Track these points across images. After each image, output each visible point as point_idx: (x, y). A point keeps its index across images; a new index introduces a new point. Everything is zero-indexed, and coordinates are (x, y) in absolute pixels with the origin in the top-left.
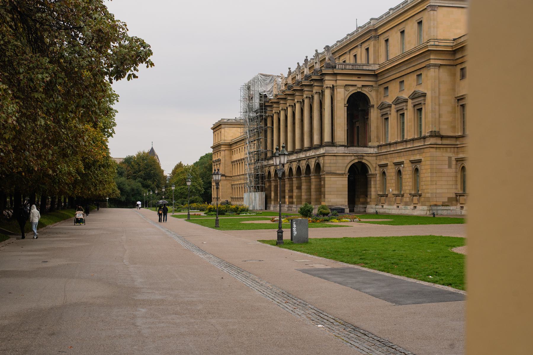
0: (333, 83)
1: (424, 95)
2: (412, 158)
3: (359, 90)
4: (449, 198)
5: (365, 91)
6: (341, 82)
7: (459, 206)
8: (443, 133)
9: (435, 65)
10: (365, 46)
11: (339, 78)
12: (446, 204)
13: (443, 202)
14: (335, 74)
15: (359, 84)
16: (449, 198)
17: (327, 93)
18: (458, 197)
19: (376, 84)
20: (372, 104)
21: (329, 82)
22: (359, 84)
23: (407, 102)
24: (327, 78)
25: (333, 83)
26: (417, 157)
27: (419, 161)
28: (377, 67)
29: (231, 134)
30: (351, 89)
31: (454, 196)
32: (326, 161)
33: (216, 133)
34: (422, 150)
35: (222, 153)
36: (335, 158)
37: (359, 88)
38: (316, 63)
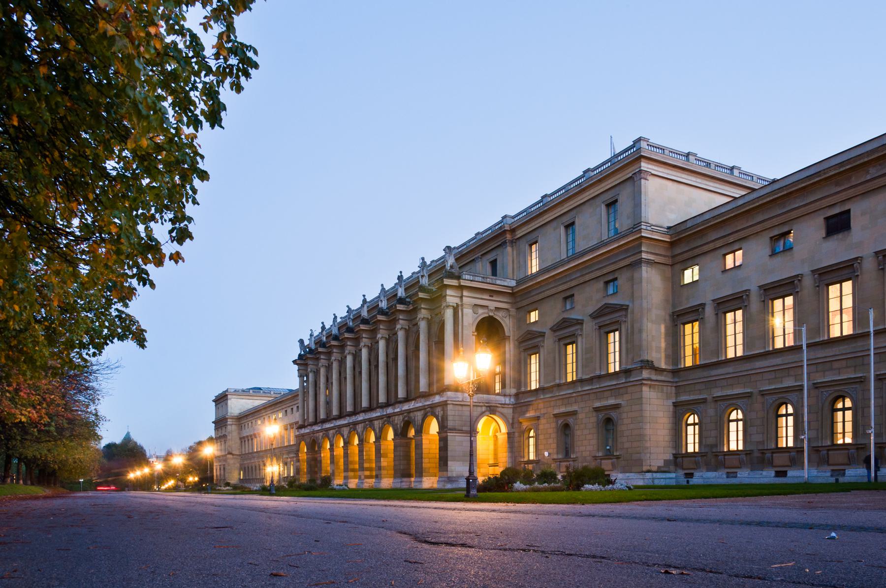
0: (457, 300)
1: (624, 308)
2: (597, 404)
3: (491, 314)
4: (665, 461)
5: (499, 316)
6: (469, 299)
7: (681, 473)
8: (656, 364)
9: (649, 262)
10: (491, 257)
11: (465, 293)
12: (663, 469)
13: (659, 467)
14: (461, 288)
15: (492, 305)
16: (665, 461)
17: (449, 314)
18: (679, 460)
19: (512, 307)
20: (507, 334)
21: (451, 297)
22: (492, 305)
23: (582, 324)
24: (449, 292)
25: (457, 300)
26: (612, 401)
27: (616, 407)
28: (513, 283)
29: (236, 406)
30: (481, 311)
31: (672, 458)
32: (449, 413)
33: (220, 406)
34: (621, 391)
35: (229, 427)
36: (460, 407)
37: (491, 310)
38: (422, 276)
